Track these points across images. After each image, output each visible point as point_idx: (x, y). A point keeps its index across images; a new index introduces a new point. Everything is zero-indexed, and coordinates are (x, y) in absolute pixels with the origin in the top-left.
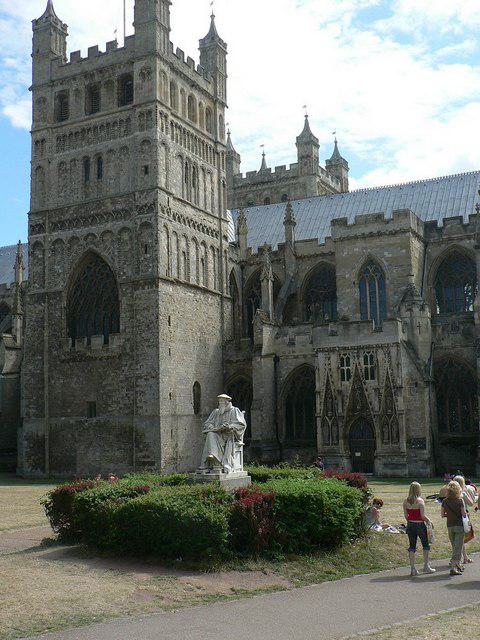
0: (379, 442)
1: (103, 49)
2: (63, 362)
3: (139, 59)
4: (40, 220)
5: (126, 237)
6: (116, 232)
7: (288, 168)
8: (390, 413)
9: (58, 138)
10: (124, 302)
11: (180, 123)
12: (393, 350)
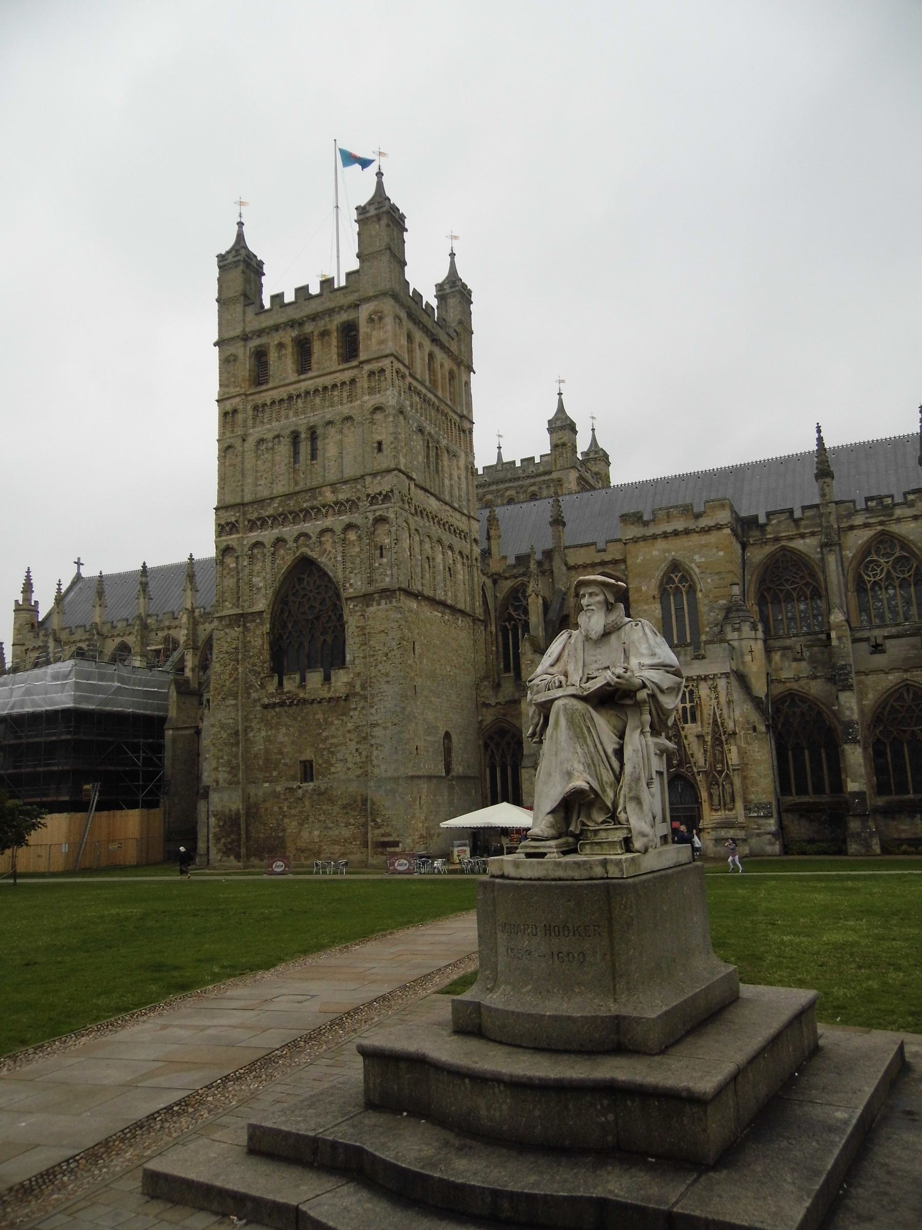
0: (706, 807)
1: (315, 290)
2: (265, 707)
3: (368, 300)
4: (232, 516)
5: (352, 536)
6: (338, 529)
7: (537, 460)
8: (718, 773)
9: (255, 408)
10: (352, 623)
11: (420, 387)
12: (722, 683)
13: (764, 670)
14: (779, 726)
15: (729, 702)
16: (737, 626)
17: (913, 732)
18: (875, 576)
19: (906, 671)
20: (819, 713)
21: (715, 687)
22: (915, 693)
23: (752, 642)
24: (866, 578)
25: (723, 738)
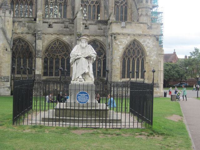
14: (14, 50)
16: (4, 11)
17: (57, 56)
19: (58, 35)
20: (28, 46)
22: (60, 42)
23: (9, 18)
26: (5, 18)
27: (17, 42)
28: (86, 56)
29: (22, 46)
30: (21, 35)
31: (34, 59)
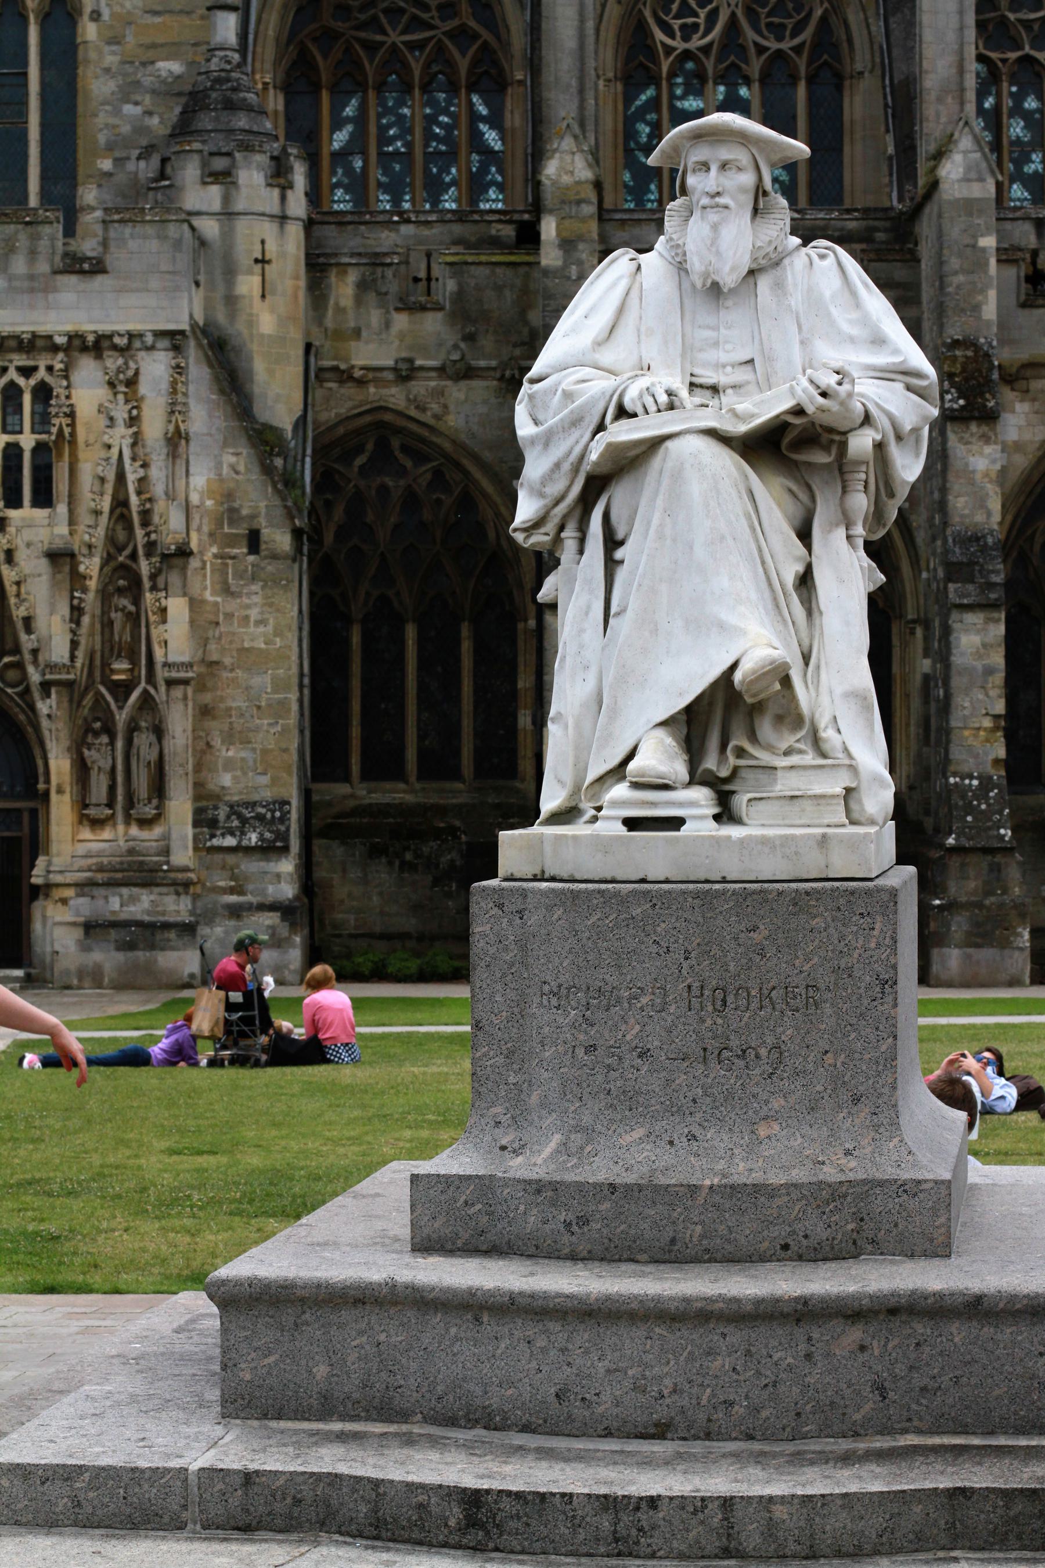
0: (61, 810)
12: (155, 369)
13: (296, 337)
14: (329, 538)
15: (176, 440)
16: (219, 164)
18: (688, 32)
21: (132, 383)
23: (268, 230)
24: (659, 35)
25: (144, 567)
26: (228, 235)
27: (360, 460)
28: (760, 408)
29: (411, 501)
30: (394, 390)
31: (532, 623)
